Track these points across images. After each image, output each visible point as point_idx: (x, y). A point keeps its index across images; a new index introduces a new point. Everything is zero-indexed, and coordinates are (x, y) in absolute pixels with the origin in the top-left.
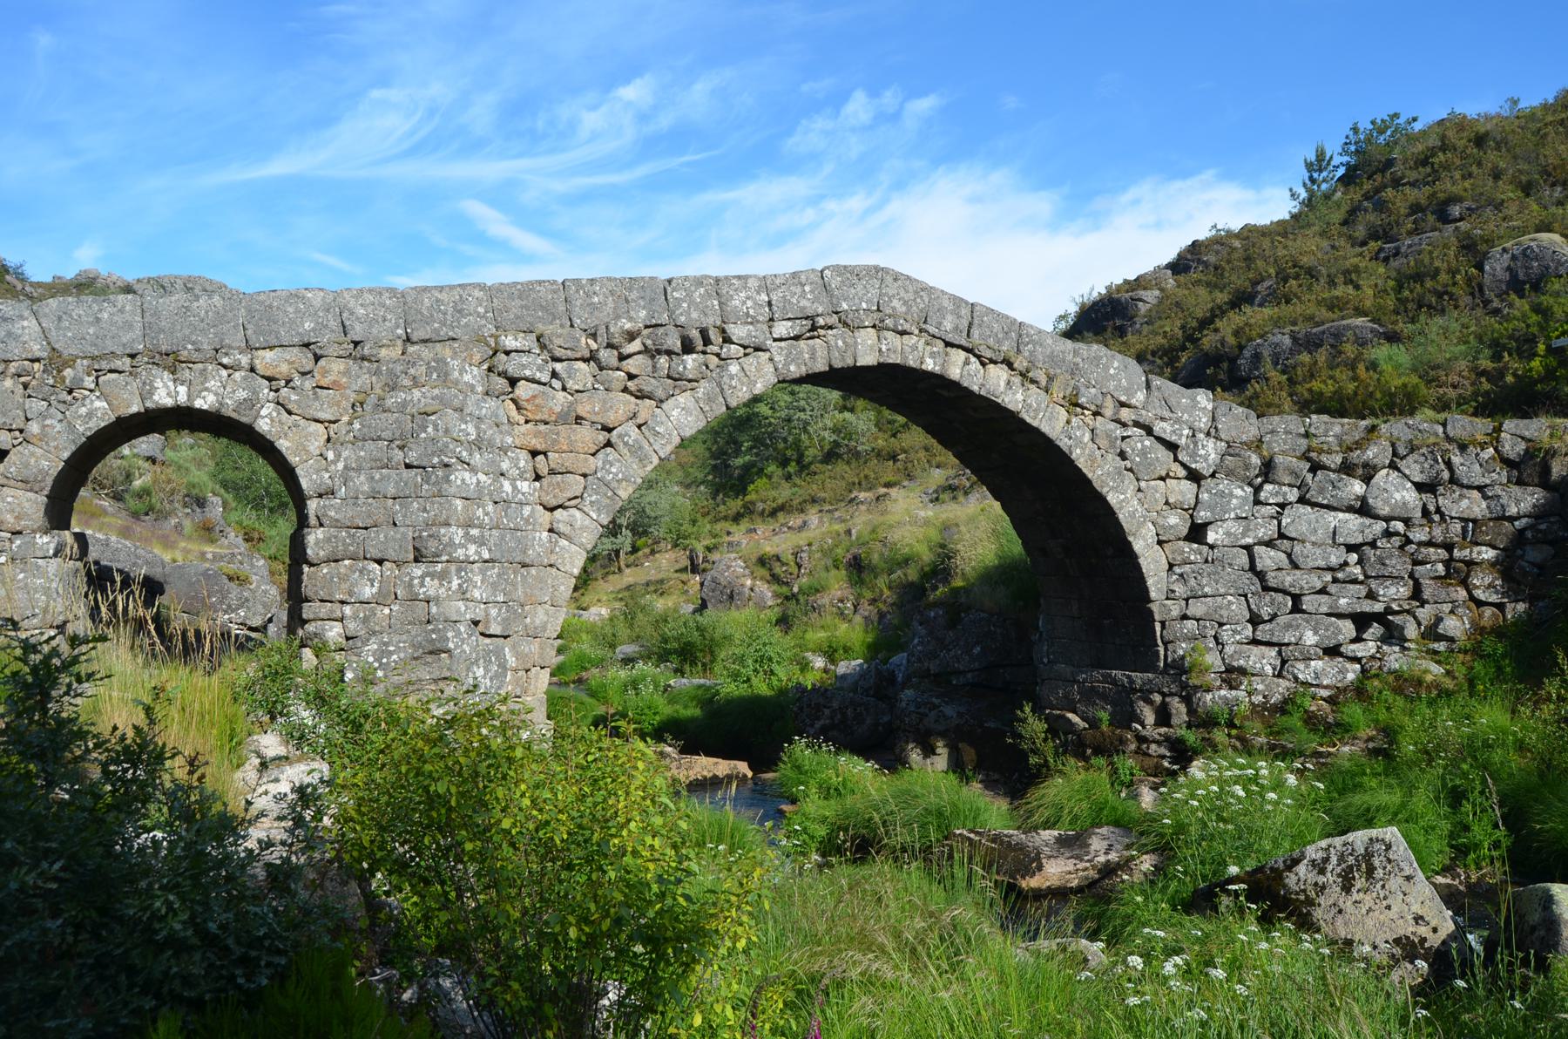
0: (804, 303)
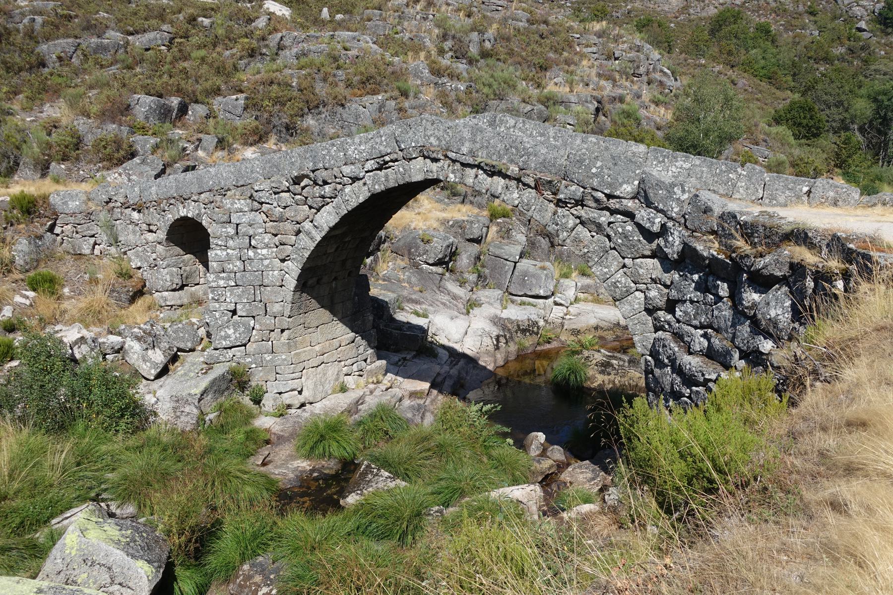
0: (382, 148)
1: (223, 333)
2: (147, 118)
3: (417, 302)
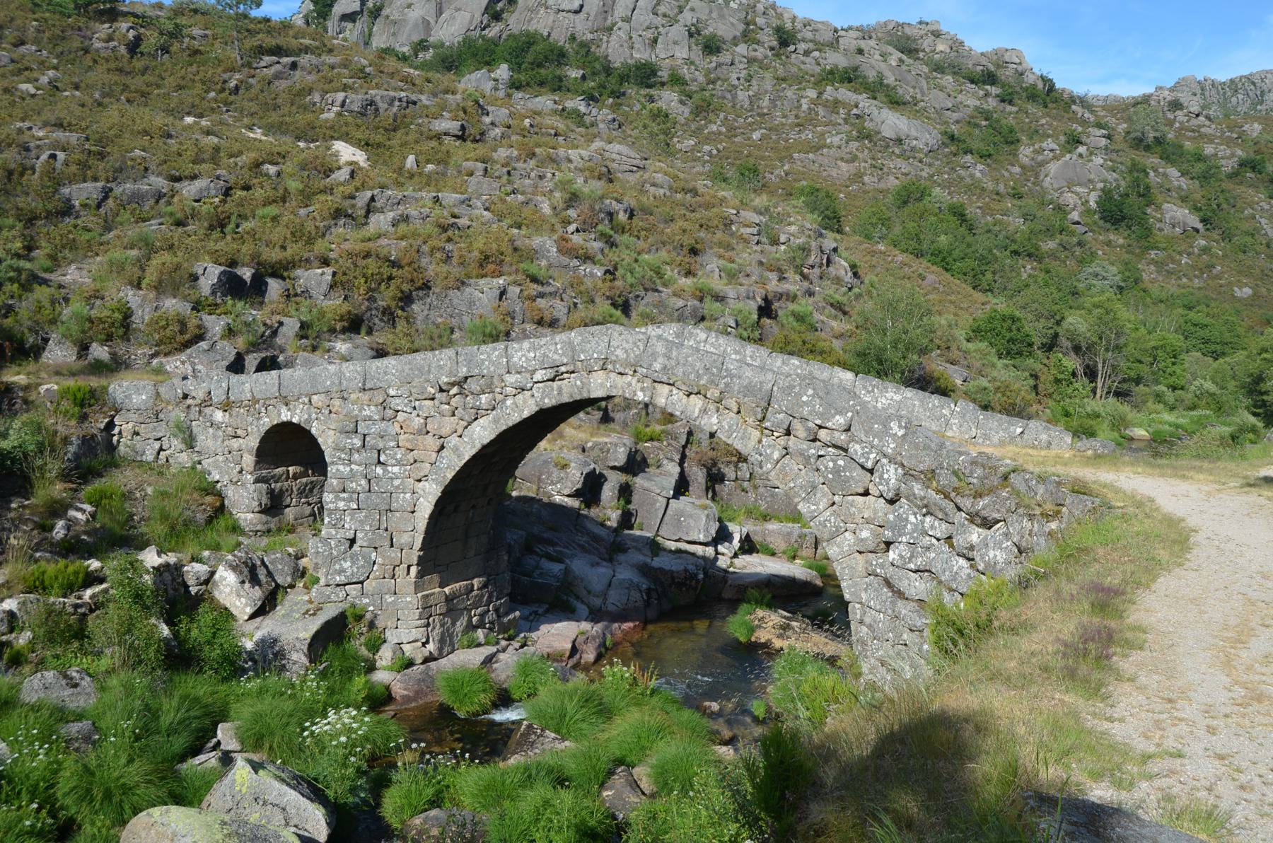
0: (556, 357)
1: (337, 567)
2: (214, 293)
3: (550, 543)
